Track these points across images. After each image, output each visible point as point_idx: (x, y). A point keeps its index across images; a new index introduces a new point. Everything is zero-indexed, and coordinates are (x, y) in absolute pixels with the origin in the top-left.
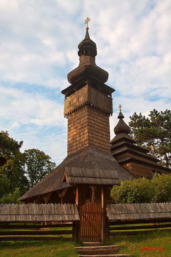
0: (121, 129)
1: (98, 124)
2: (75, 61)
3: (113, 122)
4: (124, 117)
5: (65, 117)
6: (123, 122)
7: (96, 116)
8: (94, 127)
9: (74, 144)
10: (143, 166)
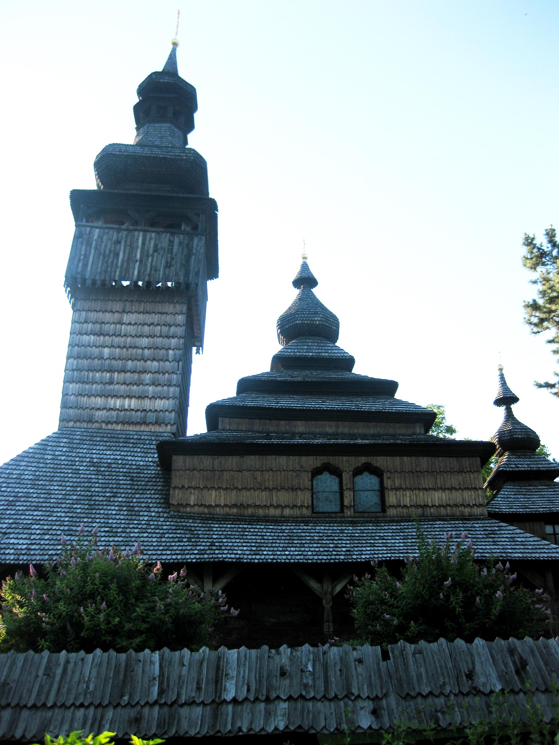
0: (309, 326)
8: (101, 358)
10: (251, 461)
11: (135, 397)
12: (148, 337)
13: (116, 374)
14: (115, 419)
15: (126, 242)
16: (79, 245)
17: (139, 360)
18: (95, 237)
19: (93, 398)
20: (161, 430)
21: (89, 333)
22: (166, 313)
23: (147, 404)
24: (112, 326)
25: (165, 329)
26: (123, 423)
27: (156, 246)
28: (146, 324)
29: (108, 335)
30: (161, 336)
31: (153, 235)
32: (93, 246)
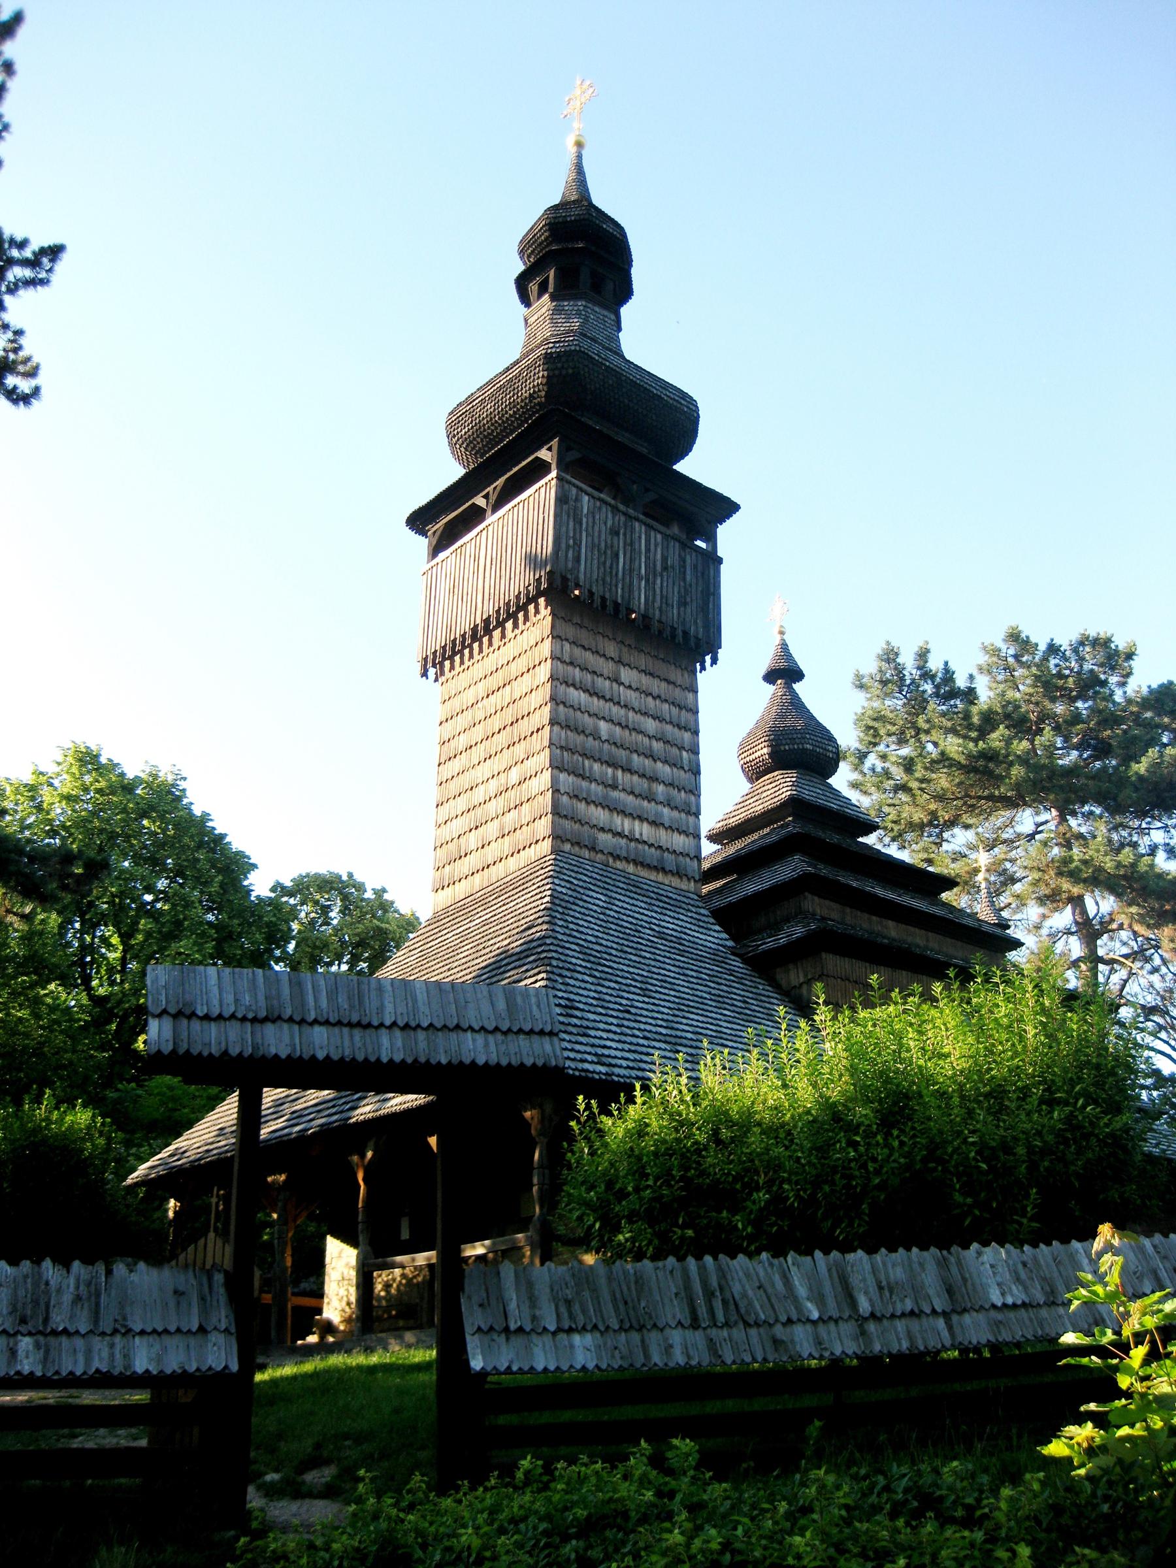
1: (622, 712)
2: (498, 336)
3: (729, 705)
4: (798, 675)
5: (425, 674)
6: (795, 704)
7: (607, 667)
8: (596, 736)
9: (473, 840)
11: (647, 820)
12: (654, 719)
13: (620, 773)
14: (624, 854)
15: (625, 534)
16: (565, 517)
17: (646, 757)
18: (585, 511)
19: (592, 807)
20: (684, 887)
21: (578, 685)
22: (674, 683)
23: (663, 837)
24: (607, 682)
25: (675, 711)
26: (635, 862)
27: (664, 559)
28: (651, 694)
29: (603, 697)
30: (671, 723)
31: (659, 536)
32: (584, 526)
